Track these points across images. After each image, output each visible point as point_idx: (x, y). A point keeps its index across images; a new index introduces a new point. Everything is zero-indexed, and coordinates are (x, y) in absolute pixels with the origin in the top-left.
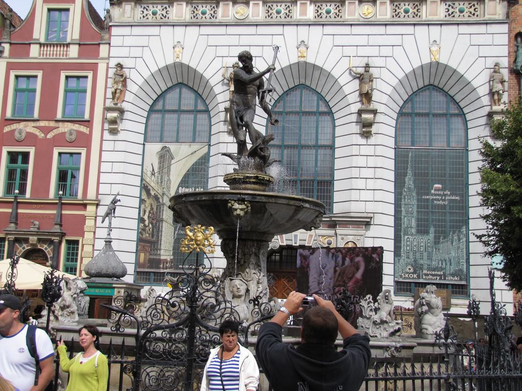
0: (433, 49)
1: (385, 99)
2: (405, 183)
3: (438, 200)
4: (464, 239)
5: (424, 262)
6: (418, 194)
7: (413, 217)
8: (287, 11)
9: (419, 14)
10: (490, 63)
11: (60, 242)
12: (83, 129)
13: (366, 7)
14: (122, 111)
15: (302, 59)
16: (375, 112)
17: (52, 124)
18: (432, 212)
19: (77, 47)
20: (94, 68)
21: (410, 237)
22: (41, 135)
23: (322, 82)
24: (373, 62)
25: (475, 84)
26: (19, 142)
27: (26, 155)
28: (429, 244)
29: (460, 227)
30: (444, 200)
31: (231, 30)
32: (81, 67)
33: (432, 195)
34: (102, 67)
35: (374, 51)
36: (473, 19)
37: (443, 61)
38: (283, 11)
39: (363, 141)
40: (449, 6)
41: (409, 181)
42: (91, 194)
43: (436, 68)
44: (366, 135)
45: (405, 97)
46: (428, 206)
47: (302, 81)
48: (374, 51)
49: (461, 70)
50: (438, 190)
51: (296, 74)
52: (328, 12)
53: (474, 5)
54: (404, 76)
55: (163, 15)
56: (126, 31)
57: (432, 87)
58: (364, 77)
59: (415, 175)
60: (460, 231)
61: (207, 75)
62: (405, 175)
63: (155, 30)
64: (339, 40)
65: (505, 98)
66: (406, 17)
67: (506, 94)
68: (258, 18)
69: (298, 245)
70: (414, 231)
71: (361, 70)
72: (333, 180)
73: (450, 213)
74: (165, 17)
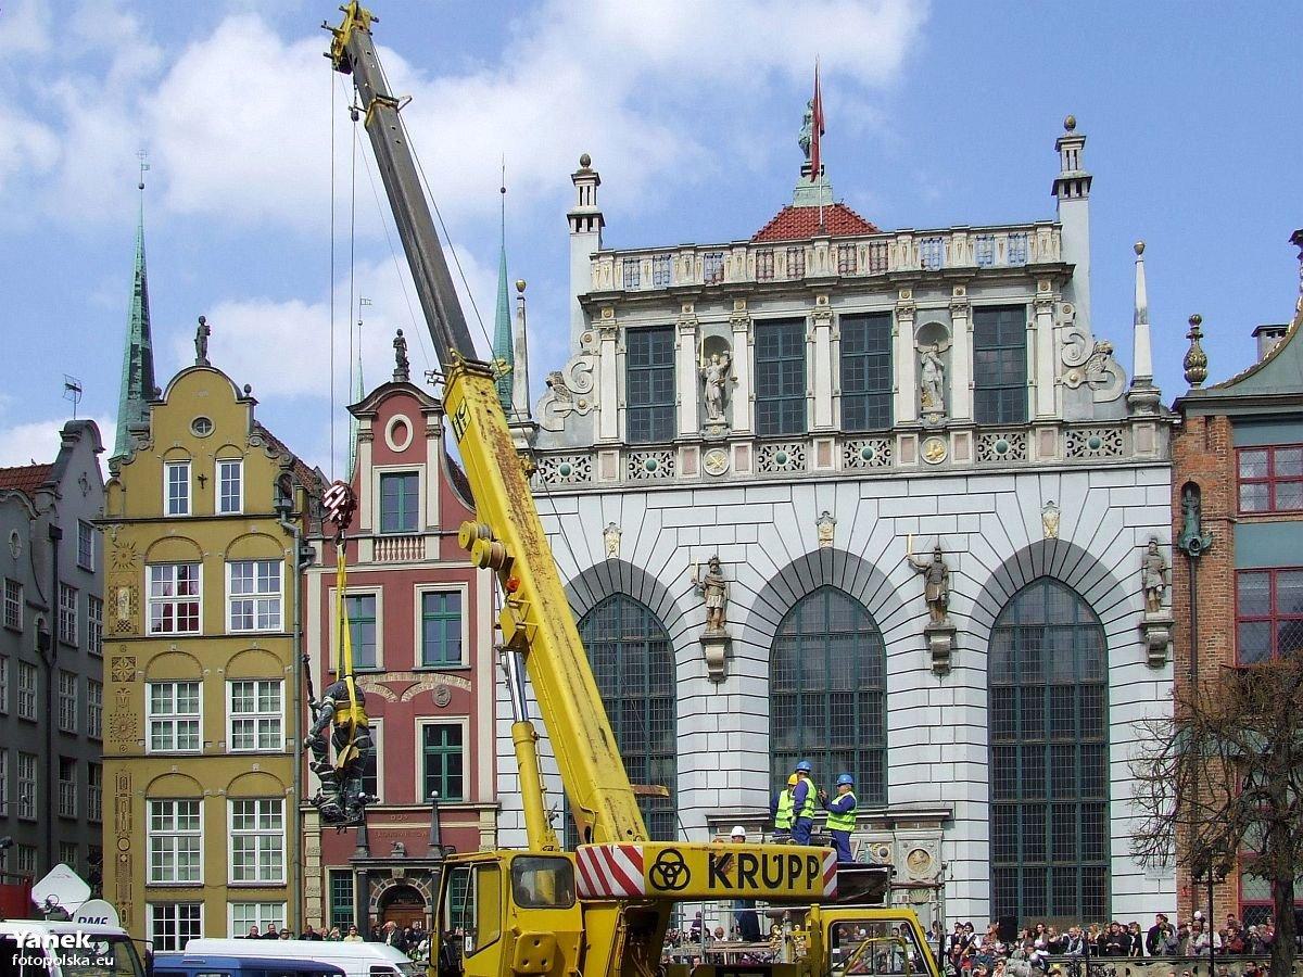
0: (1050, 515)
1: (969, 607)
8: (796, 457)
9: (1023, 452)
10: (1143, 537)
12: (460, 683)
13: (932, 444)
15: (827, 544)
16: (952, 632)
17: (408, 677)
19: (438, 538)
23: (862, 579)
24: (949, 543)
25: (1118, 574)
31: (701, 498)
35: (949, 524)
36: (1116, 459)
37: (1065, 537)
38: (789, 458)
39: (933, 681)
40: (1074, 436)
43: (1051, 548)
44: (941, 671)
45: (1003, 600)
47: (827, 580)
48: (949, 524)
49: (1095, 552)
51: (816, 569)
52: (868, 456)
53: (1115, 434)
54: (1000, 567)
55: (580, 474)
57: (1047, 579)
58: (934, 572)
61: (665, 580)
64: (888, 508)
65: (1167, 600)
66: (1002, 458)
67: (1169, 590)
68: (747, 473)
71: (927, 560)
72: (886, 748)
74: (584, 478)
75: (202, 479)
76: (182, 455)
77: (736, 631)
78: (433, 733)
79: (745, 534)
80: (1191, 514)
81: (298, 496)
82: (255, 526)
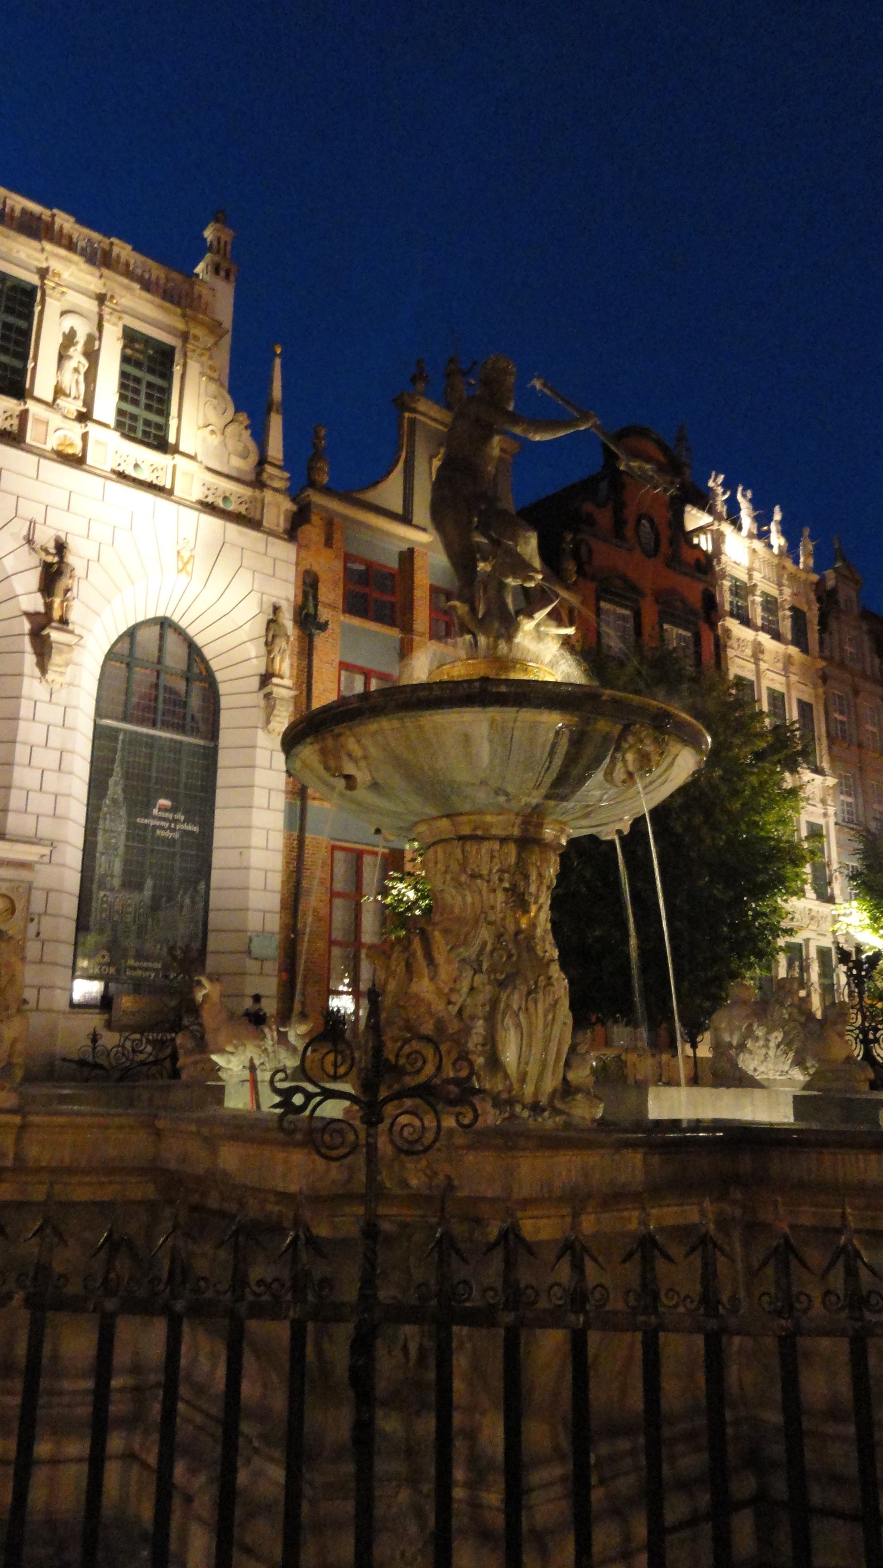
0: (186, 555)
2: (107, 789)
3: (162, 828)
4: (201, 905)
5: (131, 943)
6: (129, 814)
7: (116, 856)
18: (153, 851)
21: (108, 893)
28: (141, 910)
29: (196, 882)
30: (174, 830)
33: (154, 817)
41: (115, 787)
46: (145, 839)
50: (163, 809)
59: (127, 776)
60: (195, 888)
62: (109, 773)
70: (116, 882)
73: (182, 855)
80: (311, 598)
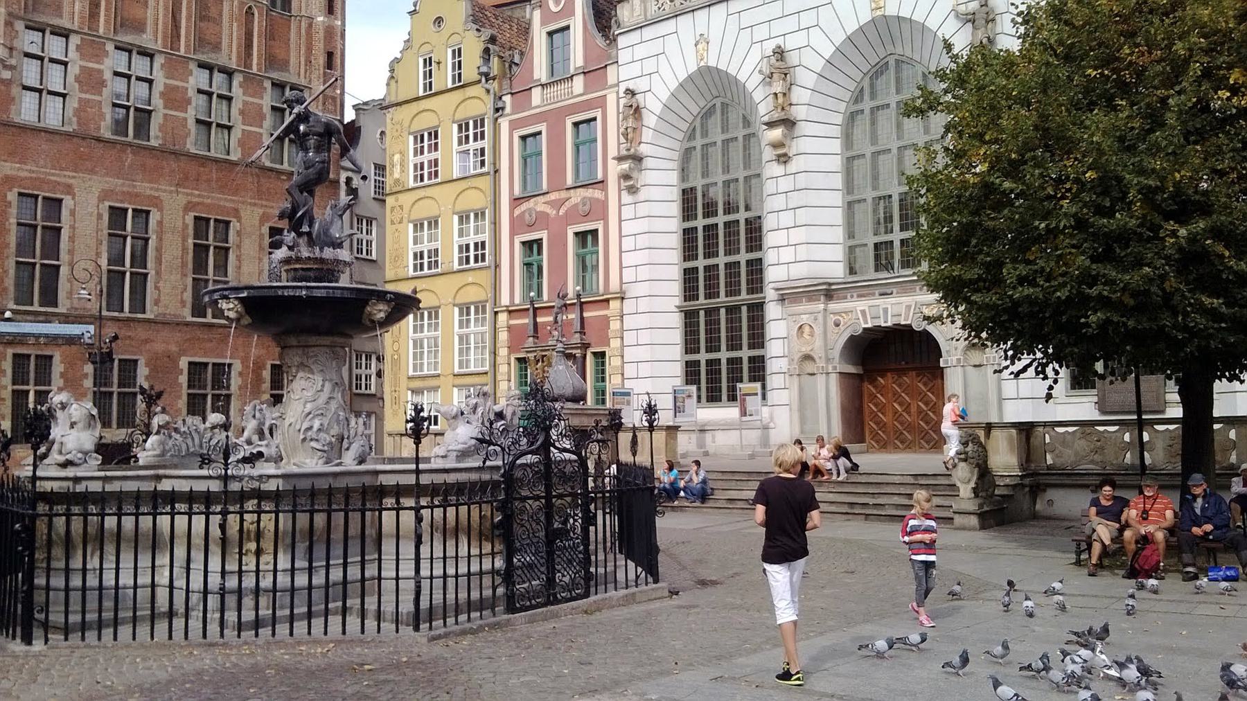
11: (584, 357)
12: (596, 193)
14: (638, 159)
15: (879, 13)
17: (564, 194)
19: (582, 77)
20: (601, 103)
22: (552, 212)
23: (917, 44)
26: (531, 227)
27: (539, 242)
32: (588, 105)
34: (611, 99)
42: (614, 285)
56: (634, 37)
61: (742, 77)
63: (669, 26)
69: (889, 324)
75: (439, 63)
76: (427, 48)
77: (799, 112)
78: (581, 236)
79: (807, 19)
81: (495, 61)
82: (471, 91)
